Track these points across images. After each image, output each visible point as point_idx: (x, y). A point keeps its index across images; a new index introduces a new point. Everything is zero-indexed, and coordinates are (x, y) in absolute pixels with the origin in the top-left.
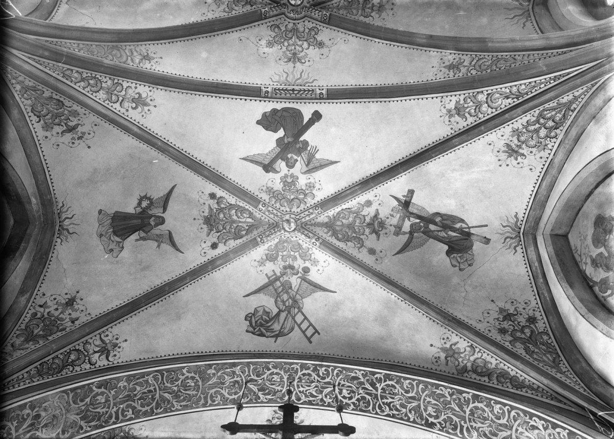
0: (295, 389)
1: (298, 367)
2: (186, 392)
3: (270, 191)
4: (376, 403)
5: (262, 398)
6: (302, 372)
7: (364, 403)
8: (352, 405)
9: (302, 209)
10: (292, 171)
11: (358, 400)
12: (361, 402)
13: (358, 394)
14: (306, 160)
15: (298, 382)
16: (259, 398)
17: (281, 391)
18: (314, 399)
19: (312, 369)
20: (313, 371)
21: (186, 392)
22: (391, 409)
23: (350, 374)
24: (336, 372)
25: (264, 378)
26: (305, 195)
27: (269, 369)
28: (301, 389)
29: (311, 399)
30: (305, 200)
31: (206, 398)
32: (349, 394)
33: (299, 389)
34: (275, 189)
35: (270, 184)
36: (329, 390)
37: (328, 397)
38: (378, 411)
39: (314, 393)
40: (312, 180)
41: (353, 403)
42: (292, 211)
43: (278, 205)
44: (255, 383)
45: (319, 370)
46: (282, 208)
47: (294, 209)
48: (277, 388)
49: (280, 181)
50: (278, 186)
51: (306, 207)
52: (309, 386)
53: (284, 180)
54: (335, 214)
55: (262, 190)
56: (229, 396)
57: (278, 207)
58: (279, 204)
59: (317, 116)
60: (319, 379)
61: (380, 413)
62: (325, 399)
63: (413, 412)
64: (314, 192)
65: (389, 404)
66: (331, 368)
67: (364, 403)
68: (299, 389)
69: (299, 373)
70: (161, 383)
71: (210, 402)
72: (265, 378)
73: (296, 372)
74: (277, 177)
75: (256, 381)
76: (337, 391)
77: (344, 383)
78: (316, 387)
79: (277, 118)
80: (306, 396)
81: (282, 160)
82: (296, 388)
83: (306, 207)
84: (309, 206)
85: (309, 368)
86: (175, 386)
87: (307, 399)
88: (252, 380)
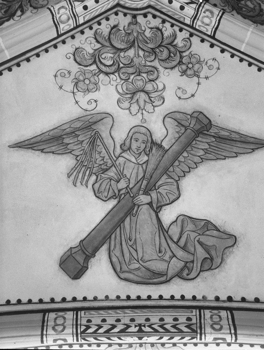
3: (189, 67)
9: (104, 22)
10: (136, 121)
14: (101, 148)
26: (96, 59)
30: (98, 46)
34: (176, 72)
35: (189, 84)
40: (83, 99)
42: (129, 18)
43: (168, 30)
46: (157, 22)
47: (123, 21)
49: (165, 94)
50: (170, 80)
51: (95, 27)
53: (154, 97)
54: (19, 13)
55: (210, 68)
57: (168, 25)
58: (166, 34)
59: (75, 263)
64: (75, 68)
74: (171, 102)
79: (180, 253)
81: (160, 146)
83: (95, 27)
84: (87, 31)
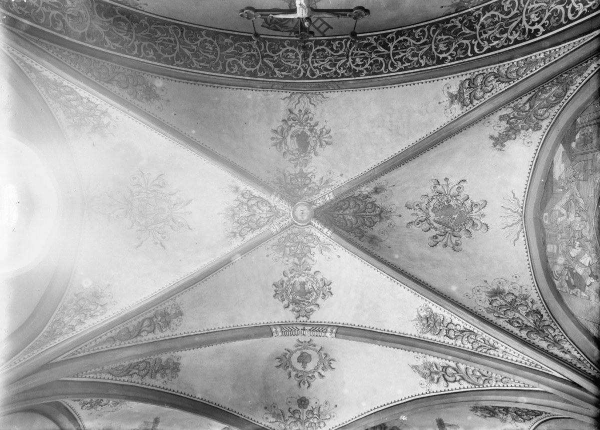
0: (309, 66)
1: (312, 44)
2: (205, 54)
4: (389, 62)
5: (277, 74)
6: (316, 49)
7: (376, 66)
8: (365, 70)
11: (371, 65)
12: (374, 66)
13: (371, 59)
15: (313, 58)
16: (275, 74)
17: (296, 68)
18: (328, 72)
19: (326, 44)
20: (327, 46)
21: (205, 54)
22: (403, 63)
23: (362, 42)
24: (349, 43)
25: (279, 55)
27: (284, 47)
28: (316, 65)
29: (325, 73)
31: (224, 65)
32: (361, 61)
33: (314, 65)
36: (343, 61)
37: (342, 68)
38: (390, 69)
39: (329, 67)
41: (367, 69)
44: (271, 59)
45: (332, 45)
48: (292, 65)
52: (323, 61)
56: (246, 68)
60: (332, 53)
61: (392, 71)
62: (339, 71)
63: (424, 57)
65: (400, 60)
66: (344, 40)
67: (376, 66)
68: (314, 65)
69: (314, 50)
70: (180, 37)
71: (228, 70)
72: (281, 55)
73: (311, 49)
75: (272, 57)
76: (350, 60)
77: (357, 52)
78: (330, 61)
80: (321, 71)
82: (311, 64)
85: (322, 44)
86: (195, 45)
87: (321, 74)
88: (268, 56)
